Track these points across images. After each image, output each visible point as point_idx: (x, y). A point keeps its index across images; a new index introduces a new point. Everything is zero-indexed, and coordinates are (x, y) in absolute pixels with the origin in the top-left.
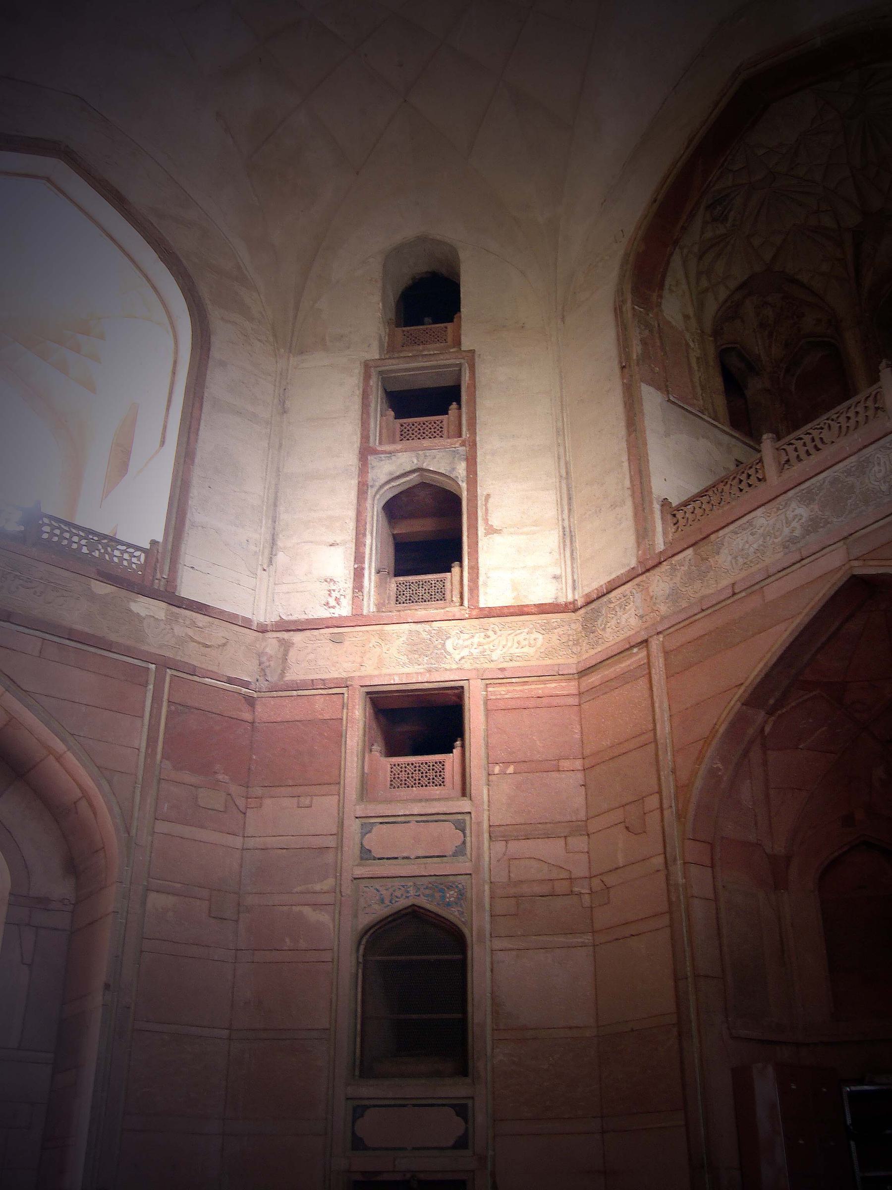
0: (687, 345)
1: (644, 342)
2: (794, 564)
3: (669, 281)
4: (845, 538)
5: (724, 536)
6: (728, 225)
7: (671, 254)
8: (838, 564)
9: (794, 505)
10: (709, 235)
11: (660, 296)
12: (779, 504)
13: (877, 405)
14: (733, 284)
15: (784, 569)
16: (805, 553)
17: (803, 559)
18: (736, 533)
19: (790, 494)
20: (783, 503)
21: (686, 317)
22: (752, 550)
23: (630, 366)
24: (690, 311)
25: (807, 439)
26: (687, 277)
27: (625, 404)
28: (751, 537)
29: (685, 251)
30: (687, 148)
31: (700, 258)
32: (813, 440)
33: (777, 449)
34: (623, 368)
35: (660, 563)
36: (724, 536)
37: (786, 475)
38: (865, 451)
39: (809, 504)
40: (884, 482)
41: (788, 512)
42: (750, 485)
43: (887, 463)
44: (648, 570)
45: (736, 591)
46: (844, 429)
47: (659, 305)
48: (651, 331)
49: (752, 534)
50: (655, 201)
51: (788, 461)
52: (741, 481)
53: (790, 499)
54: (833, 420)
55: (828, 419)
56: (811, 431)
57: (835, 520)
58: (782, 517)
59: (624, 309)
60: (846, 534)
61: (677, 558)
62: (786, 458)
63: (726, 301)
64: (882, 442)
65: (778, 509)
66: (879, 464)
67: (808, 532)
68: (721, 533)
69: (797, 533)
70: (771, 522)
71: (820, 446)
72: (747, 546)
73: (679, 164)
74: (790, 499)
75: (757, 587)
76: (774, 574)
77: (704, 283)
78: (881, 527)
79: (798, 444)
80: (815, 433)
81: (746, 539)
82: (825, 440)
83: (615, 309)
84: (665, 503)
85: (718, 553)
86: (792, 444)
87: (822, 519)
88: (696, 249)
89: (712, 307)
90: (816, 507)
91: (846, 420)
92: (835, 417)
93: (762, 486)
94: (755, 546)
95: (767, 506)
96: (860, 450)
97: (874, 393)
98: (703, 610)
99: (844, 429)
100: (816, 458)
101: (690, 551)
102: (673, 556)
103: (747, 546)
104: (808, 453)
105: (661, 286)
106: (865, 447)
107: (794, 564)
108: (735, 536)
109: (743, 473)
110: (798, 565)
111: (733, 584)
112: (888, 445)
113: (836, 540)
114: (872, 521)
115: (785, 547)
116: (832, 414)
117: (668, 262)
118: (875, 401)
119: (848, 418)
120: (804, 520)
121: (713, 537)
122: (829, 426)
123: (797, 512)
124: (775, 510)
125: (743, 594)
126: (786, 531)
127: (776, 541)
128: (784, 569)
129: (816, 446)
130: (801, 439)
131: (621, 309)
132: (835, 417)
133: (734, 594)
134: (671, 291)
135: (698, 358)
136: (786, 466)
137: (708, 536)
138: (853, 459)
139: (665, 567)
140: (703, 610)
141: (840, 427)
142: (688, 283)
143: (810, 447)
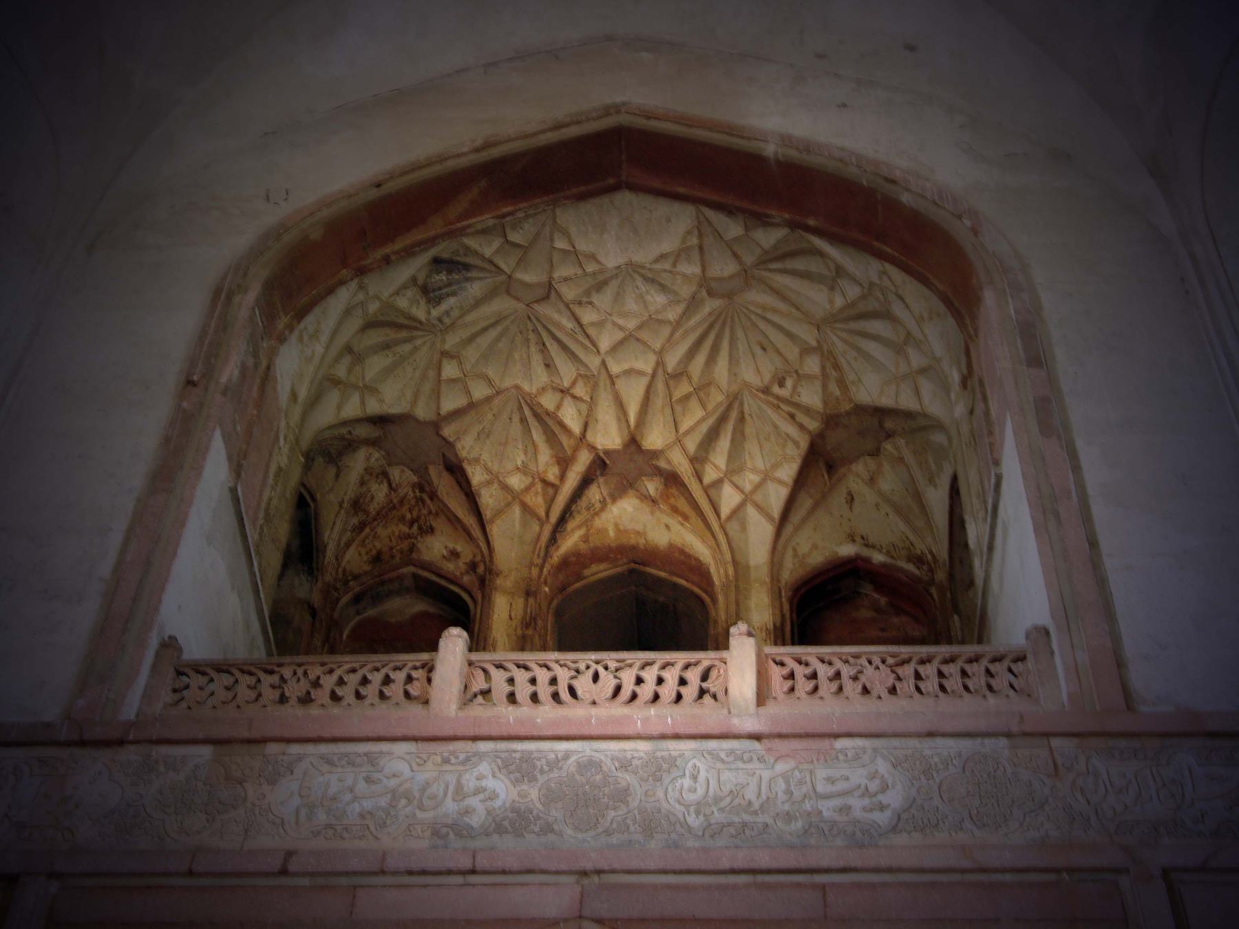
0: (277, 439)
1: (243, 368)
2: (450, 872)
3: (309, 320)
4: (584, 873)
5: (300, 758)
6: (435, 313)
7: (342, 283)
8: (551, 912)
9: (484, 768)
10: (402, 303)
11: (291, 328)
12: (453, 753)
13: (704, 685)
14: (373, 407)
15: (424, 872)
16: (482, 863)
17: (473, 872)
18: (330, 763)
19: (483, 746)
20: (462, 756)
21: (294, 396)
22: (356, 807)
23: (206, 389)
24: (303, 393)
25: (543, 676)
26: (332, 339)
27: (167, 440)
28: (362, 785)
29: (361, 296)
30: (477, 150)
31: (370, 325)
32: (554, 681)
33: (470, 664)
34: (190, 383)
35: (121, 742)
36: (300, 758)
37: (479, 710)
38: (672, 745)
39: (517, 780)
40: (698, 813)
41: (467, 776)
42: (382, 696)
43: (713, 783)
44: (83, 743)
45: (292, 868)
46: (626, 693)
47: (282, 339)
48: (256, 366)
49: (368, 780)
50: (379, 186)
51: (486, 693)
52: (365, 681)
53: (481, 756)
54: (606, 668)
55: (597, 663)
56: (553, 665)
57: (569, 832)
58: (452, 779)
59: (237, 299)
60: (589, 866)
61: (164, 750)
62: (485, 686)
63: (345, 423)
64: (712, 744)
65: (446, 761)
66: (695, 778)
67: (500, 829)
68: (295, 749)
69: (476, 821)
70: (422, 777)
71: (565, 695)
72: (348, 797)
73: (451, 164)
74: (481, 756)
75: (344, 881)
76: (395, 873)
77: (341, 371)
78: (669, 886)
79: (521, 677)
80: (563, 675)
81: (349, 782)
82: (579, 693)
83: (218, 292)
84: (170, 645)
85: (272, 782)
86: (505, 669)
87: (539, 818)
88: (373, 307)
89: (326, 416)
90: (534, 794)
91: (633, 680)
92: (613, 665)
93: (415, 709)
94: (368, 804)
95: (421, 745)
96: (663, 737)
97: (706, 663)
98: (191, 873)
99: (626, 693)
100: (546, 714)
101: (206, 751)
102: (160, 742)
103: (348, 797)
104: (534, 698)
105: (301, 315)
106: (677, 737)
107: (450, 872)
108: (326, 768)
109: (377, 670)
110: (459, 879)
111: (289, 854)
112: (723, 755)
113: (564, 867)
114: (660, 865)
115: (436, 833)
116: (611, 658)
117: (331, 291)
118: (705, 677)
119: (639, 681)
120: (498, 803)
121: (272, 748)
122: (596, 677)
123: (490, 783)
124: (439, 759)
125: (305, 882)
126: (450, 806)
127: (420, 815)
128: (424, 872)
129: (556, 696)
130: (526, 668)
131: (229, 298)
132: (613, 665)
133: (284, 872)
134: (301, 339)
135: (280, 469)
136: (480, 699)
137: (265, 741)
138: (643, 746)
139: (130, 754)
140: (191, 873)
141: (618, 689)
142: (327, 348)
143: (544, 691)
